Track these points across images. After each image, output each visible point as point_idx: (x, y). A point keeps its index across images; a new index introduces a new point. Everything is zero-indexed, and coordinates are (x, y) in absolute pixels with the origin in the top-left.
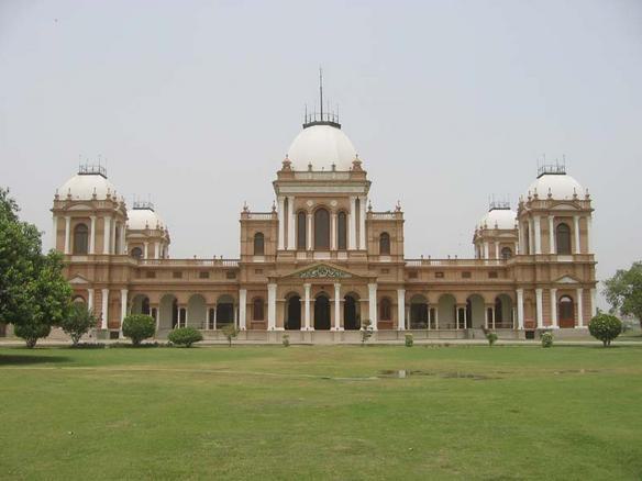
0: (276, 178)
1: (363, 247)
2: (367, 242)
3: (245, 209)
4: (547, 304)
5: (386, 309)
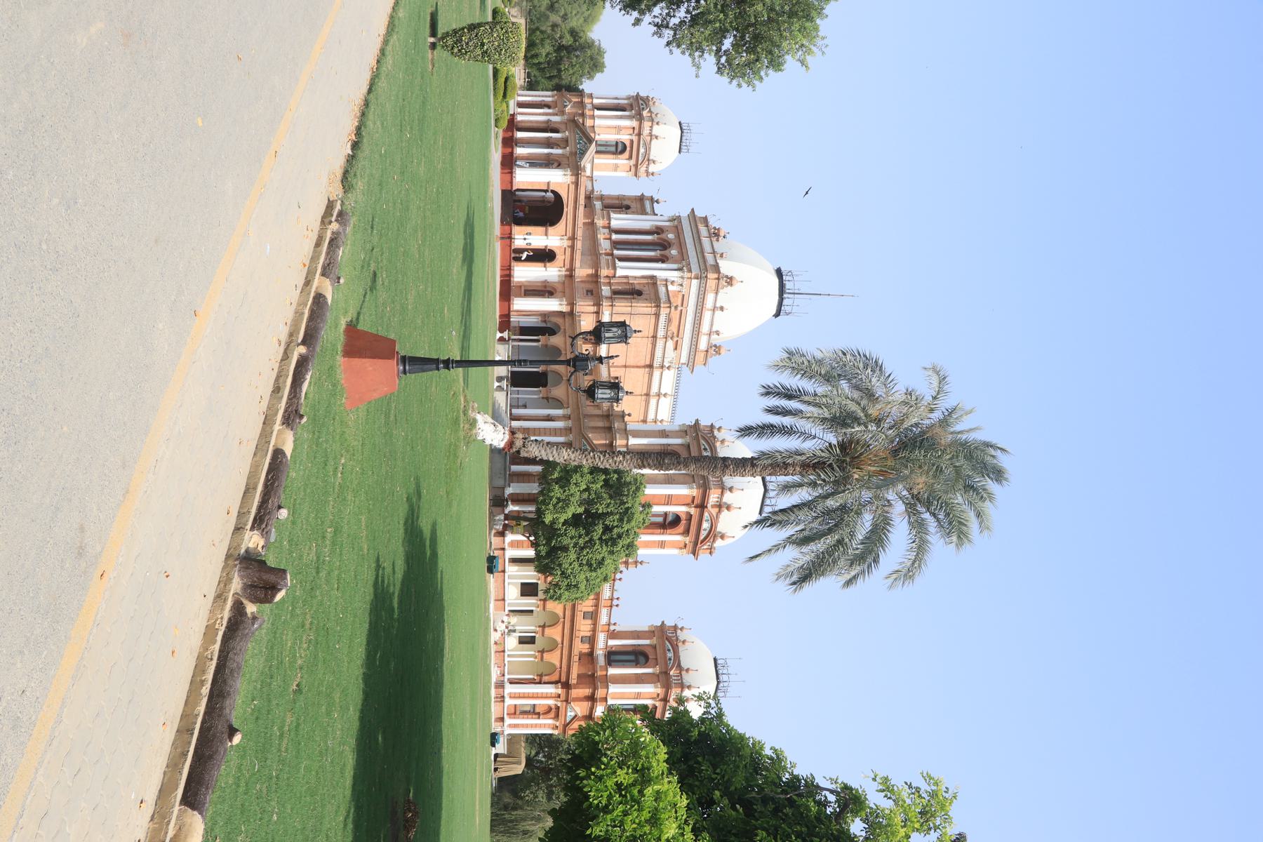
0: (699, 214)
1: (620, 272)
2: (627, 277)
4: (555, 432)
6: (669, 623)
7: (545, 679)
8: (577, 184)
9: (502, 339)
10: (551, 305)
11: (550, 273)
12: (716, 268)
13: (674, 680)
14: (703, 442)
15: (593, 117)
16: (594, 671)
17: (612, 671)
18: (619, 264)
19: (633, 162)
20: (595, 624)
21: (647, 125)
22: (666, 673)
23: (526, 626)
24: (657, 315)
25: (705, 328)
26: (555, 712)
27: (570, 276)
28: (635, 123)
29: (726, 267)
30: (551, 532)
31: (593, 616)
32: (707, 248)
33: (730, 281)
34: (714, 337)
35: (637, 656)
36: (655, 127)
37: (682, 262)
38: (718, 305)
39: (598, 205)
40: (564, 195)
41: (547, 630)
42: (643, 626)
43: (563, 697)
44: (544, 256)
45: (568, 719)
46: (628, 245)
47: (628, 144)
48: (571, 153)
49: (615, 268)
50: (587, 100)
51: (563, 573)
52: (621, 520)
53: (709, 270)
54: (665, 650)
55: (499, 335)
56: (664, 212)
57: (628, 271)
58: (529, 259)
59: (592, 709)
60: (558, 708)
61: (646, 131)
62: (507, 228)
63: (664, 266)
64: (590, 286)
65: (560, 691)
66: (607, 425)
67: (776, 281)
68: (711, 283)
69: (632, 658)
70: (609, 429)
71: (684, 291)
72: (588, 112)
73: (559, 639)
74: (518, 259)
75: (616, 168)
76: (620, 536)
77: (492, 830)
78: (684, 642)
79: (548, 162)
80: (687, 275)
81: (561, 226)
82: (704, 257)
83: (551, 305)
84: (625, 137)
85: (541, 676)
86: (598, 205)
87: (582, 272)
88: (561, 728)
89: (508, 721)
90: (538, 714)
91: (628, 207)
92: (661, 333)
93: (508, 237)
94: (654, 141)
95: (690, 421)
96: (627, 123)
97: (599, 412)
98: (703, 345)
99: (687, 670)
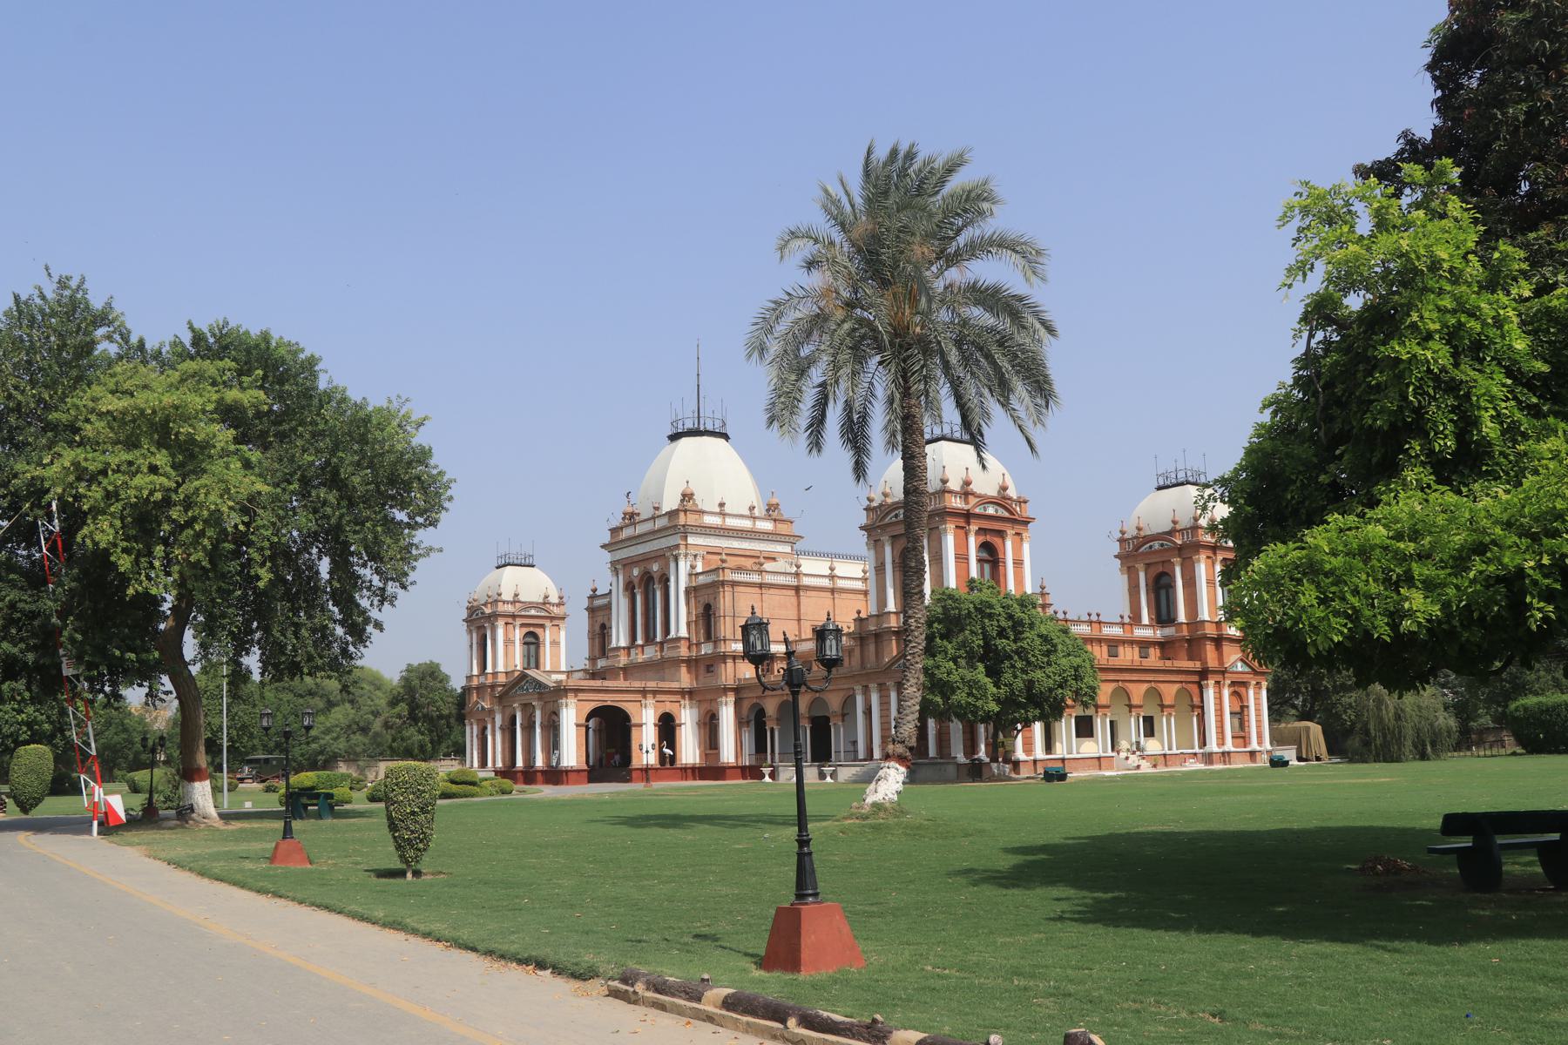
0: (607, 539)
1: (683, 633)
2: (688, 624)
3: (595, 590)
4: (885, 704)
5: (709, 727)
6: (1116, 548)
7: (1196, 701)
8: (577, 691)
9: (773, 775)
10: (727, 715)
11: (687, 718)
12: (673, 514)
13: (1188, 538)
14: (887, 520)
15: (495, 674)
16: (1183, 639)
17: (1182, 617)
18: (673, 634)
19: (548, 623)
20: (1123, 642)
21: (501, 608)
22: (1180, 550)
23: (1132, 728)
24: (734, 584)
25: (746, 524)
26: (1238, 688)
27: (690, 694)
28: (500, 623)
29: (670, 502)
30: (1009, 703)
31: (1113, 644)
32: (647, 527)
33: (687, 496)
34: (757, 512)
35: (1161, 587)
36: (505, 597)
37: (668, 557)
38: (717, 510)
39: (601, 663)
40: (591, 706)
41: (1135, 701)
42: (1122, 581)
43: (1219, 677)
44: (667, 728)
45: (1247, 669)
46: (649, 623)
47: (526, 630)
48: (539, 699)
49: (678, 639)
50: (475, 682)
51: (1061, 686)
52: (990, 616)
53: (677, 523)
54: (1151, 552)
55: (767, 779)
56: (606, 581)
57: (681, 626)
58: (672, 746)
59: (1232, 640)
60: (1233, 684)
61: (509, 608)
62: (634, 774)
63: (672, 579)
64: (702, 669)
65: (1211, 682)
66: (872, 640)
67: (684, 440)
68: (691, 519)
69: (1163, 593)
70: (878, 636)
71: (702, 552)
72: (490, 681)
73: (1145, 686)
74: (673, 759)
75: (555, 643)
76: (1010, 617)
77: (1398, 760)
78: (1139, 529)
79: (553, 729)
80: (682, 551)
81: (629, 708)
82: (659, 530)
83: (727, 715)
84: (518, 634)
85: (1193, 707)
86: (601, 663)
87: (685, 679)
88: (1259, 678)
89: (1254, 746)
90: (1242, 707)
91: (603, 627)
92: (755, 578)
93: (646, 772)
94: (522, 598)
95: (862, 537)
96: (500, 632)
97: (857, 651)
98: (767, 526)
99: (1175, 522)
